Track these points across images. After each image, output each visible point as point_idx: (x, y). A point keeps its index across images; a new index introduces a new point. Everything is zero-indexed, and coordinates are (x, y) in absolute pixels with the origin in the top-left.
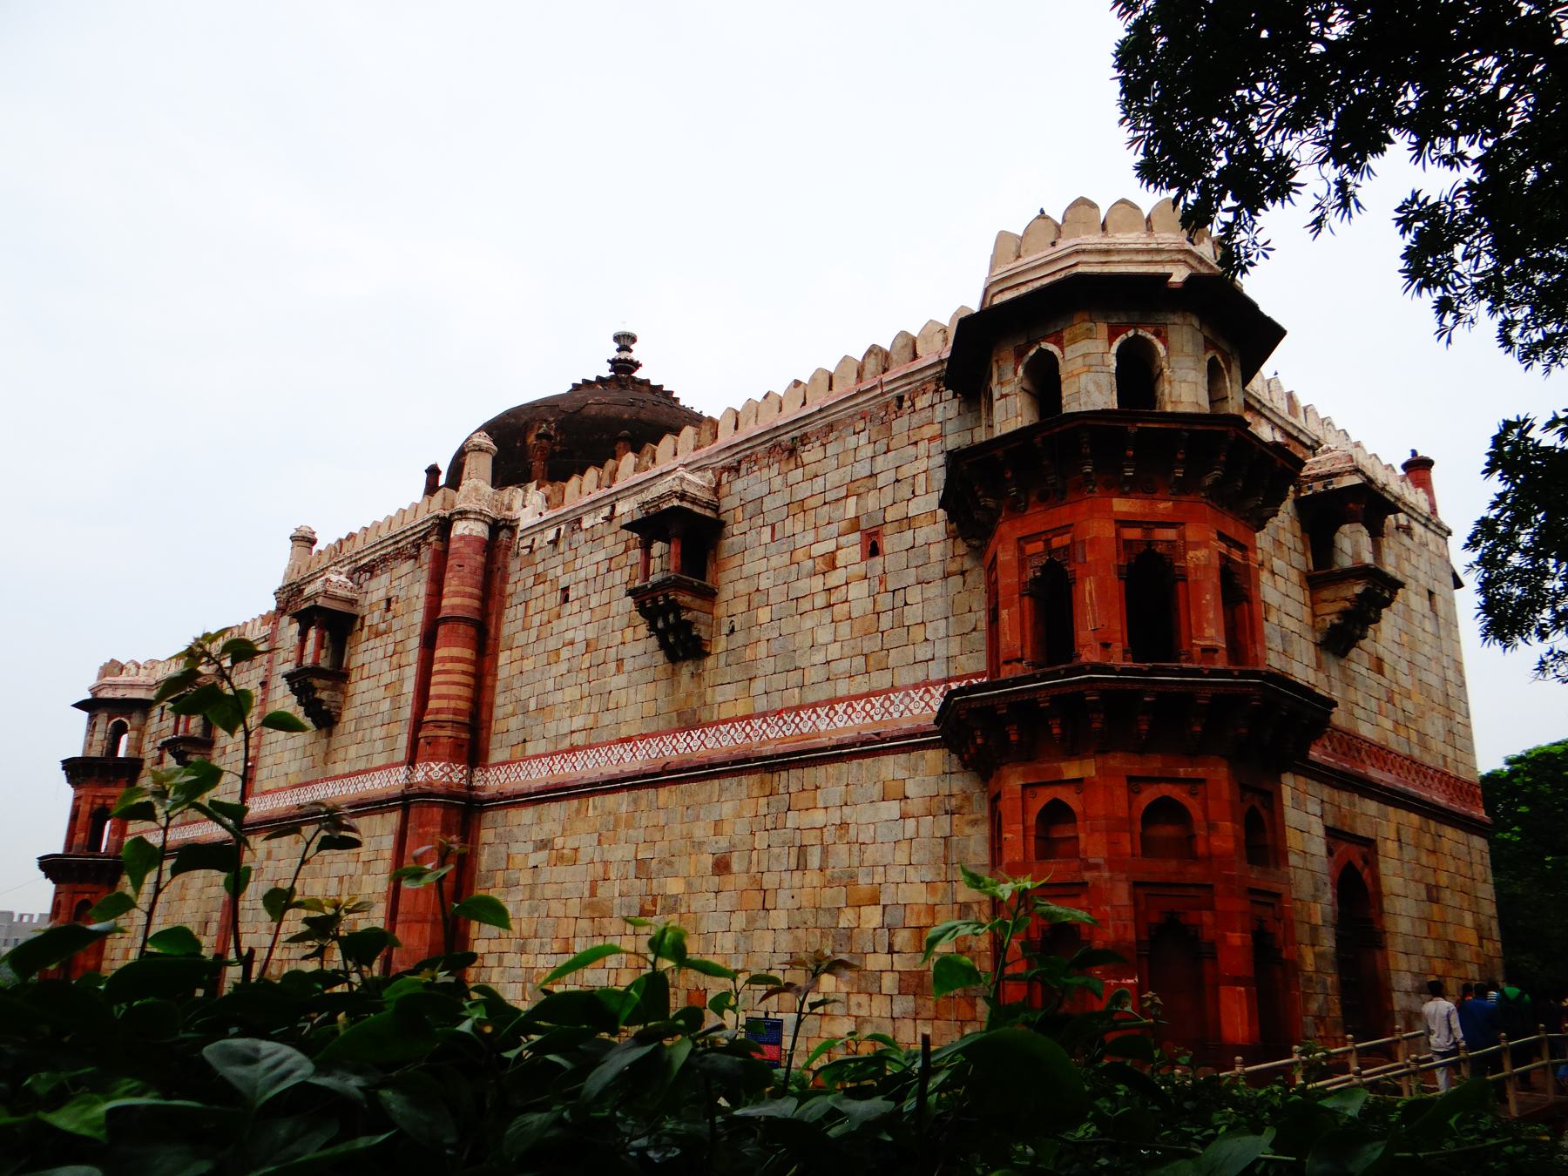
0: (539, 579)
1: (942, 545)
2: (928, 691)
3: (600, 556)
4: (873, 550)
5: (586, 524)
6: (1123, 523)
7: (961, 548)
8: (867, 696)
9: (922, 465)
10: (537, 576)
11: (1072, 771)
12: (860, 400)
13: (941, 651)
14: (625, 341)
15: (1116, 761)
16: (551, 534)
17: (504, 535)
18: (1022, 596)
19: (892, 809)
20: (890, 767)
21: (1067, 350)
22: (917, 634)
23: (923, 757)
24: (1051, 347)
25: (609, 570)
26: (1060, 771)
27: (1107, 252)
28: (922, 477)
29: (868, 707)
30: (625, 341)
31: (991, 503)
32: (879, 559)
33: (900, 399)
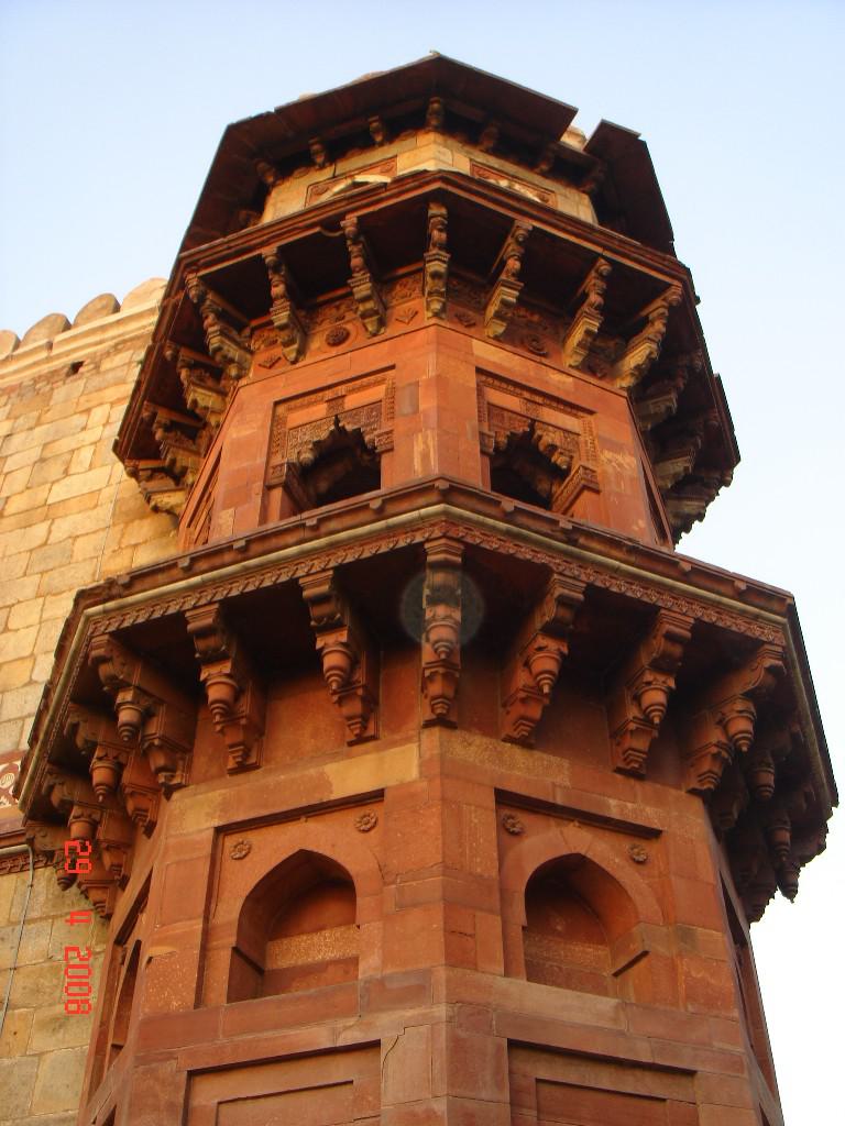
9: (90, 436)
11: (353, 774)
15: (472, 749)
18: (269, 488)
26: (328, 785)
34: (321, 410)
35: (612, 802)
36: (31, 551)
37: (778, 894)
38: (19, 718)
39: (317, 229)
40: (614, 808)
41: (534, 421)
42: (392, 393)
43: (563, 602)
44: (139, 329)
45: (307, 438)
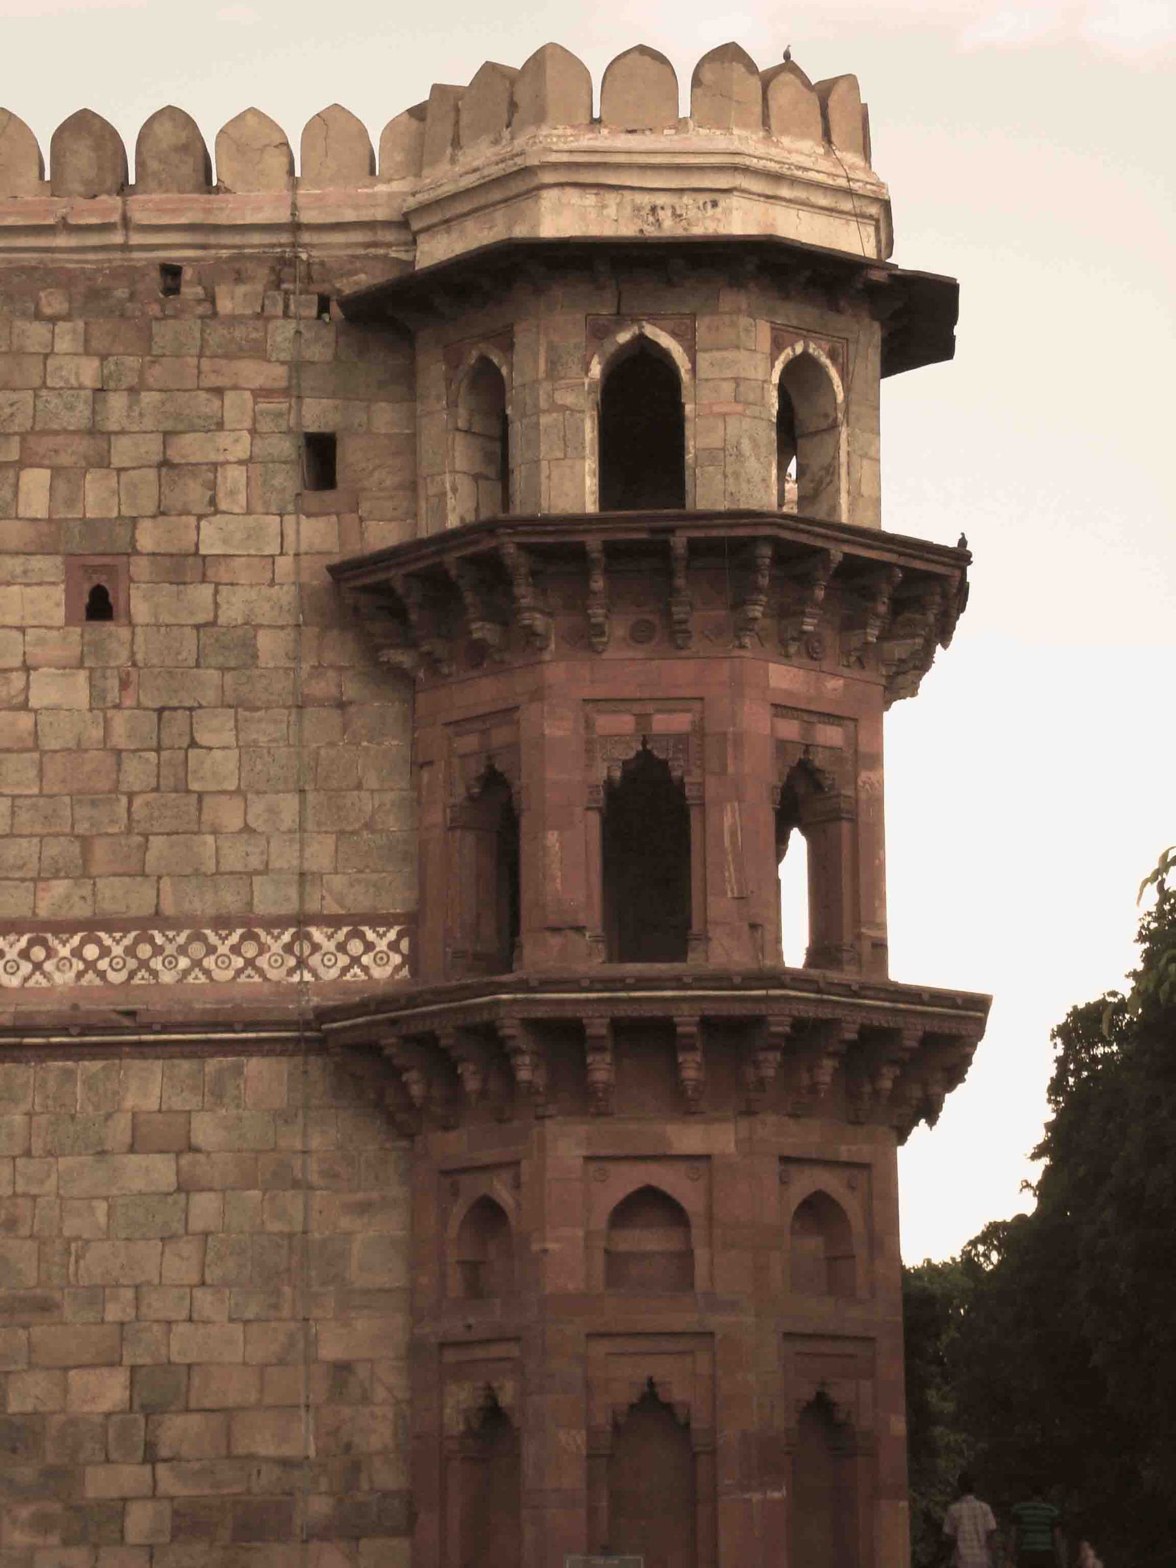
1: (287, 636)
2: (250, 936)
4: (100, 606)
6: (781, 710)
7: (340, 649)
8: (91, 926)
11: (689, 1138)
12: (61, 241)
13: (285, 857)
19: (161, 1171)
20: (147, 1087)
21: (703, 359)
22: (230, 816)
23: (238, 1071)
24: (665, 340)
27: (777, 178)
28: (235, 476)
29: (91, 951)
31: (539, 622)
32: (109, 626)
33: (171, 273)
34: (625, 723)
35: (843, 1148)
36: (198, 627)
37: (922, 1122)
38: (246, 873)
39: (644, 536)
40: (844, 1152)
41: (807, 746)
42: (700, 730)
43: (843, 1042)
44: (265, 246)
45: (616, 755)
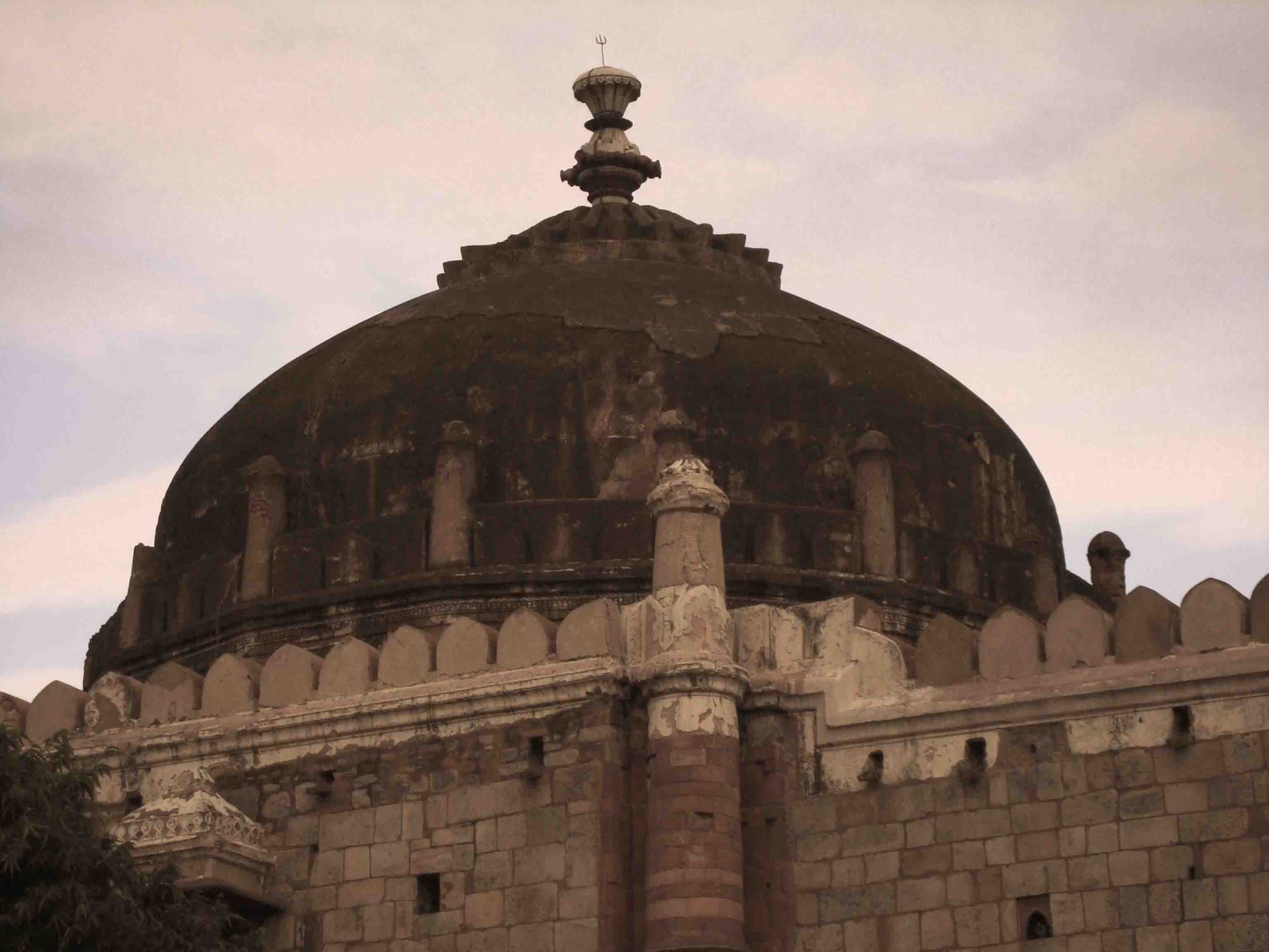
0: (913, 861)
3: (1161, 832)
5: (1087, 738)
10: (911, 855)
14: (607, 97)
16: (946, 755)
17: (766, 726)
25: (1193, 873)
30: (607, 97)
